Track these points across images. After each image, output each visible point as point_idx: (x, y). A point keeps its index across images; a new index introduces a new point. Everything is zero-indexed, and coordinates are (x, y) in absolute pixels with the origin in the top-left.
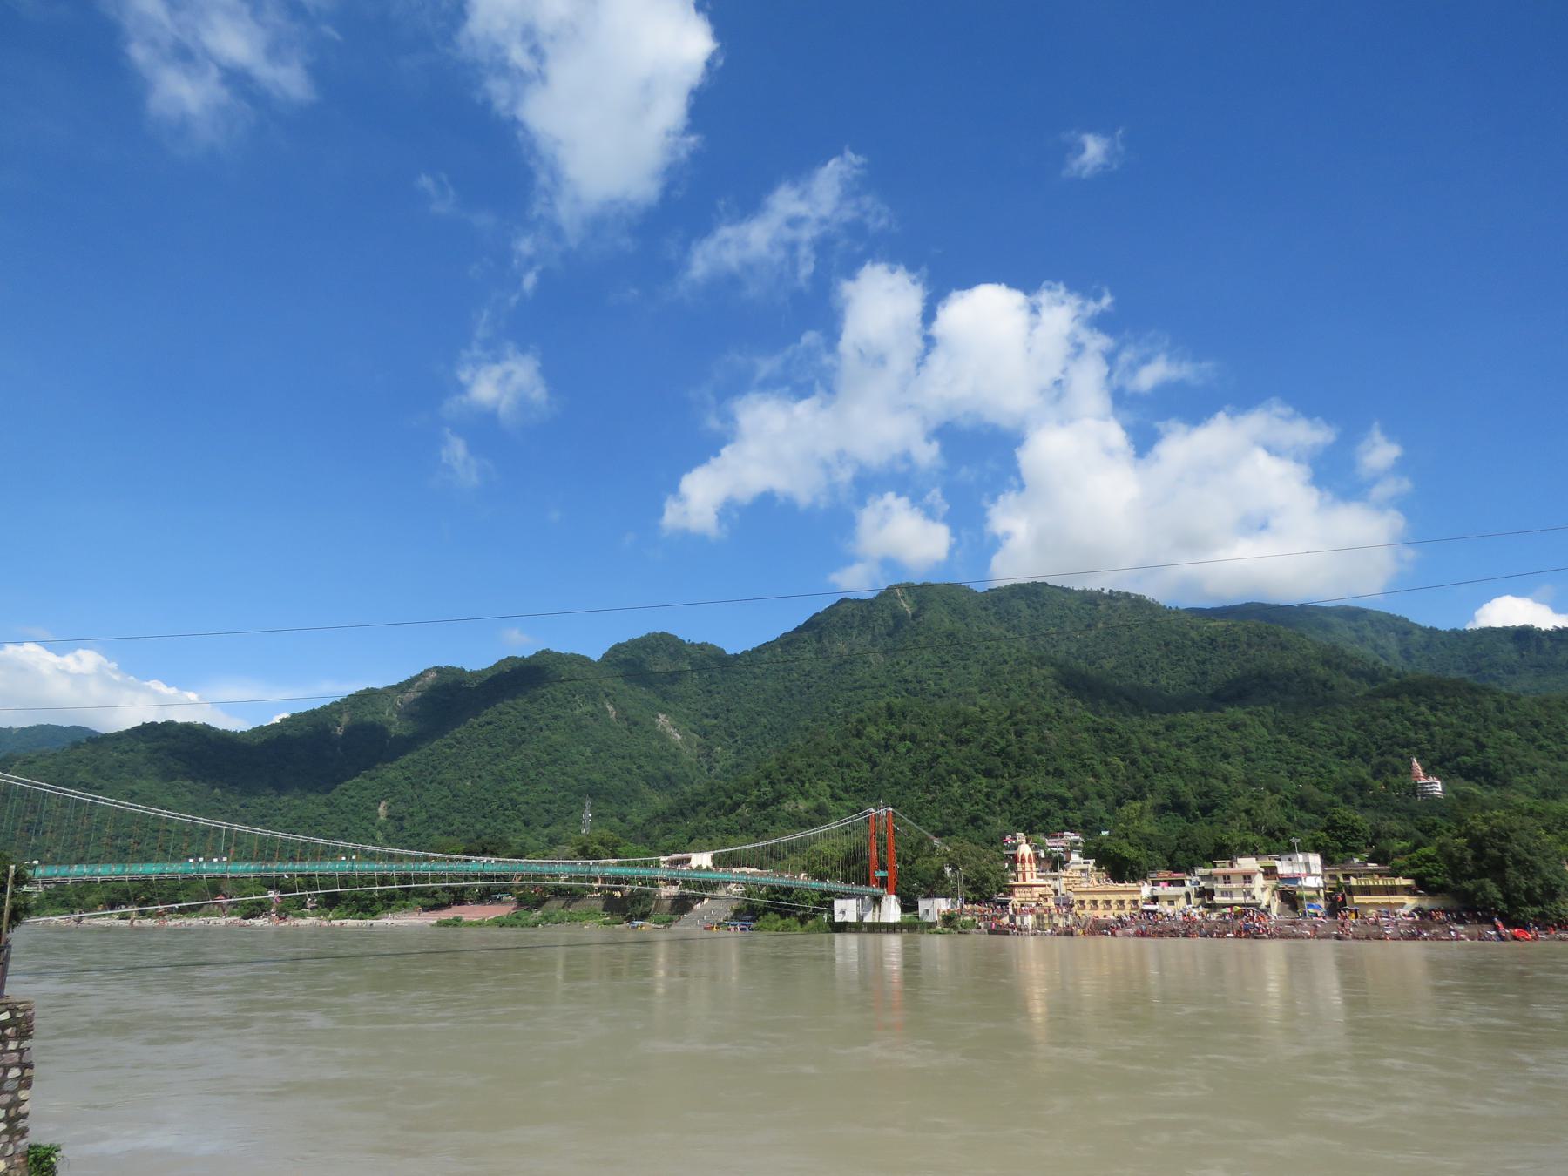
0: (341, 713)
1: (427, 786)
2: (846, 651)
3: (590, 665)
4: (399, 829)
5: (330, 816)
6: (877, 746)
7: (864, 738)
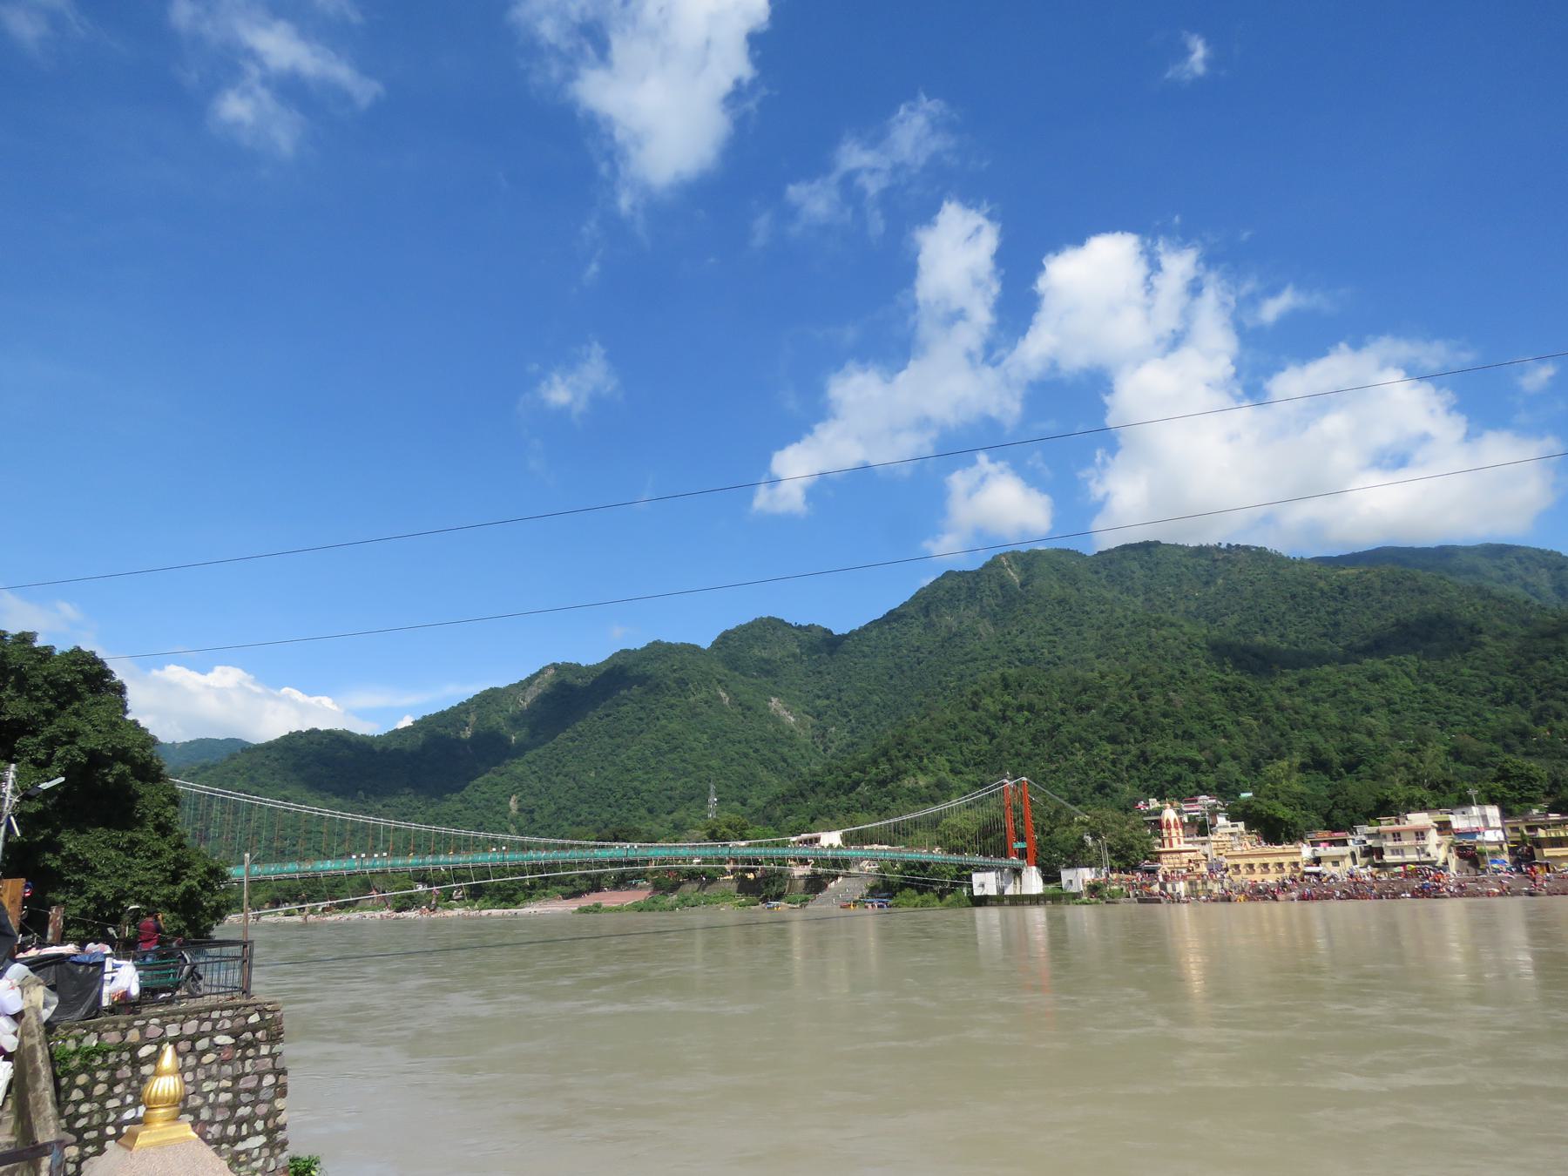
0: (468, 713)
1: (554, 779)
2: (955, 624)
3: (701, 653)
5: (464, 812)
6: (995, 718)
7: (980, 710)
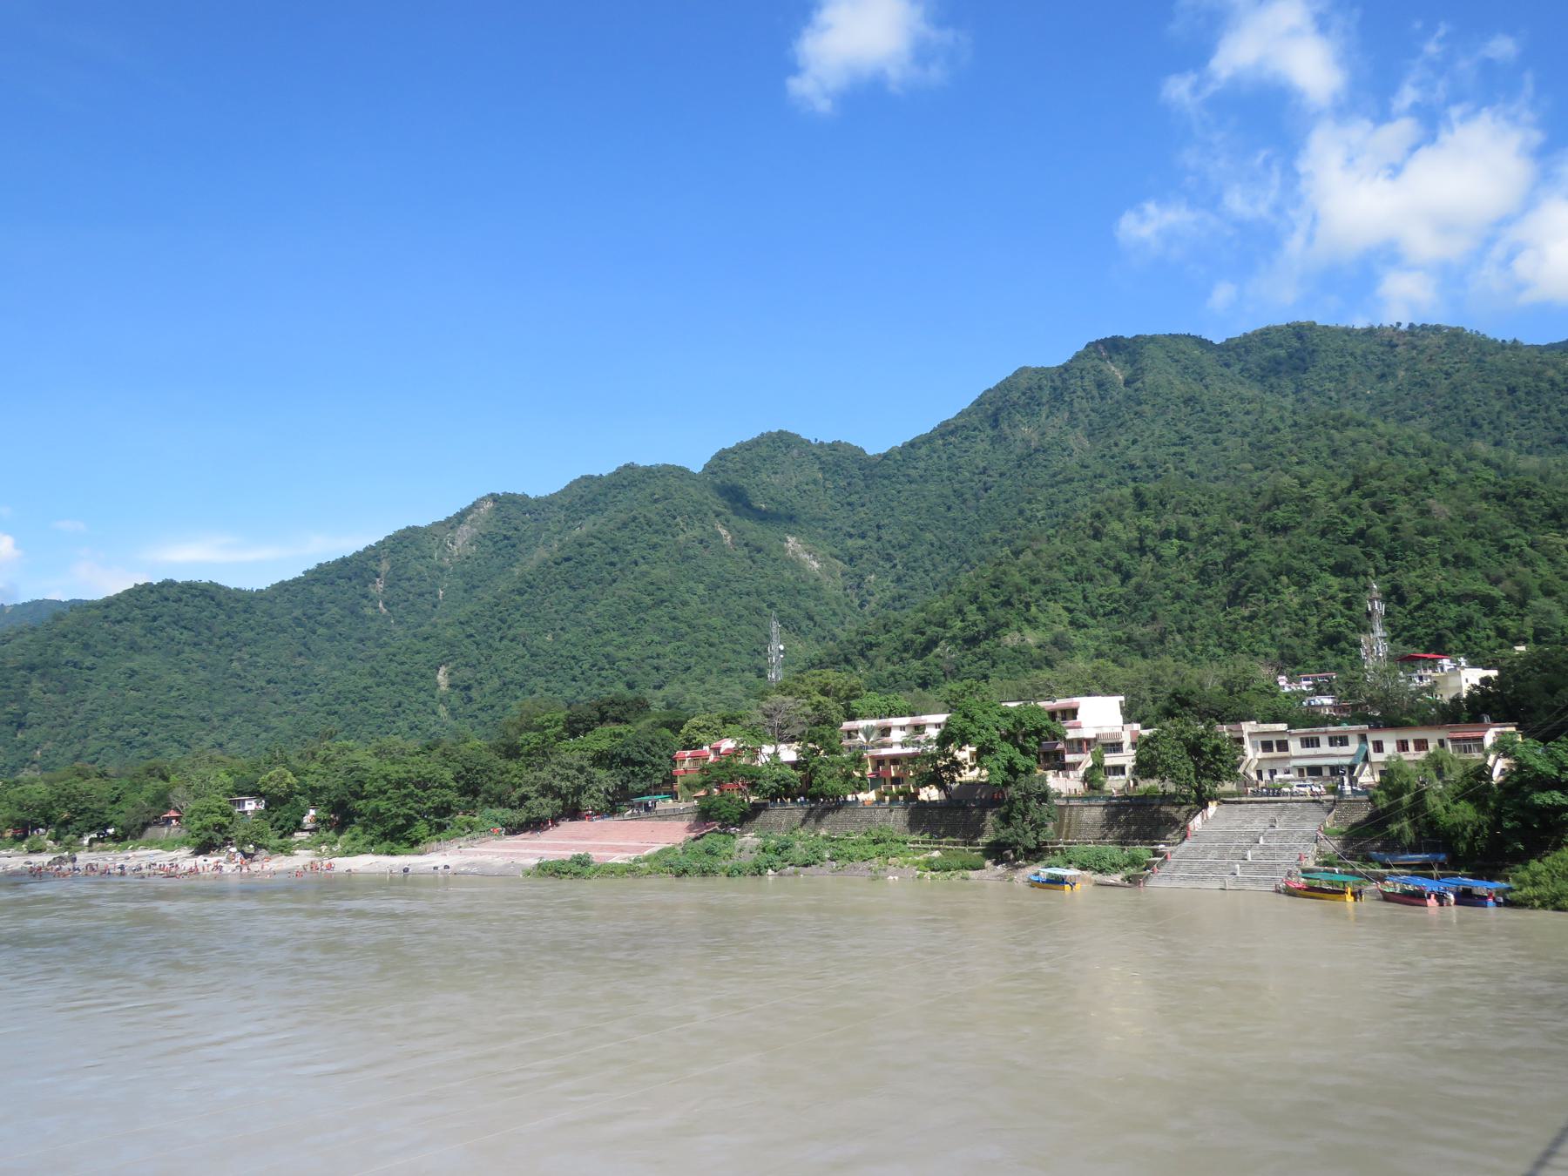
0: (379, 560)
1: (496, 644)
2: (1035, 436)
4: (465, 700)
6: (1129, 549)
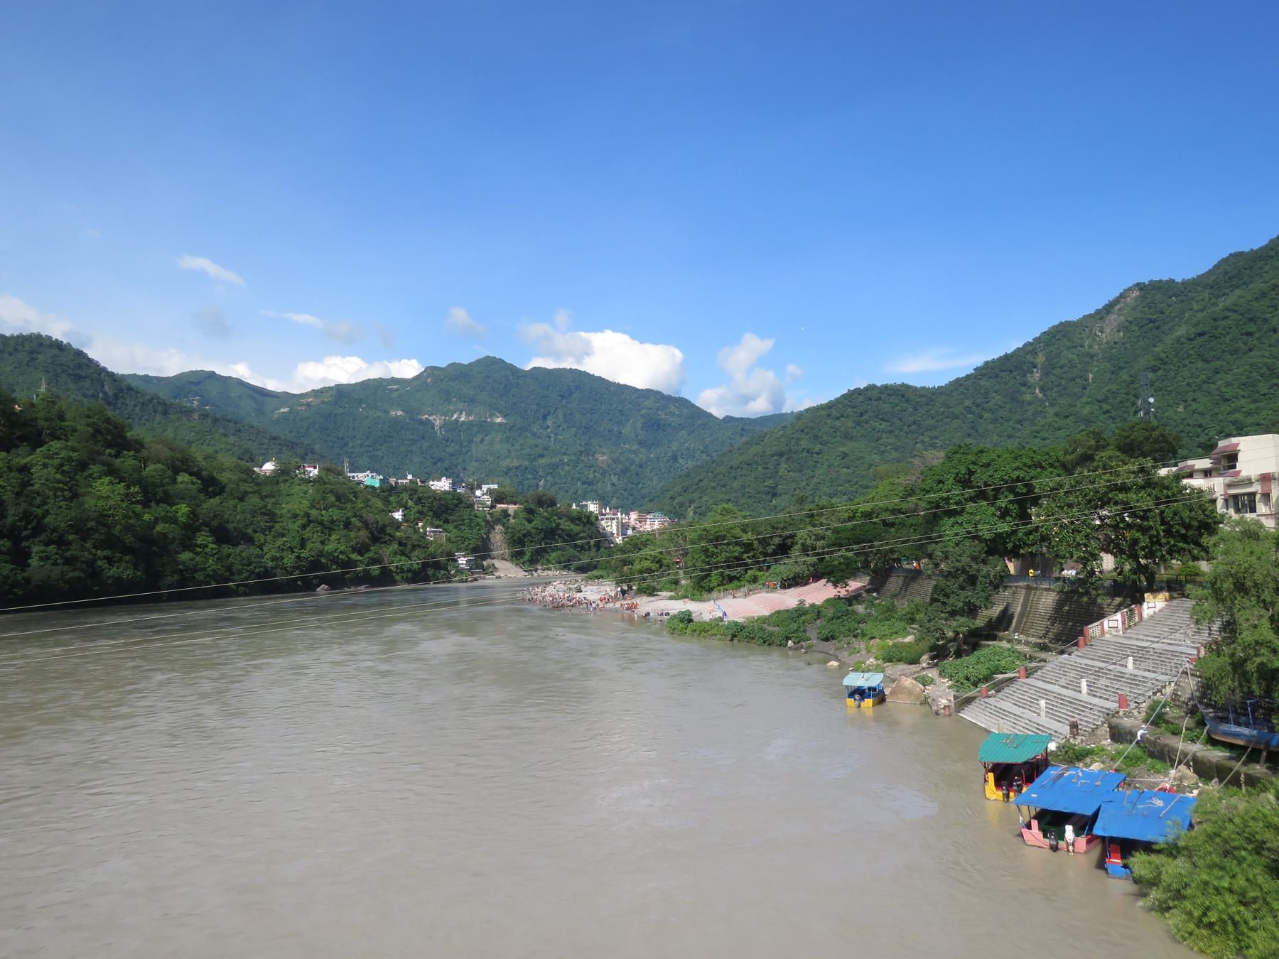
0: (1036, 353)
